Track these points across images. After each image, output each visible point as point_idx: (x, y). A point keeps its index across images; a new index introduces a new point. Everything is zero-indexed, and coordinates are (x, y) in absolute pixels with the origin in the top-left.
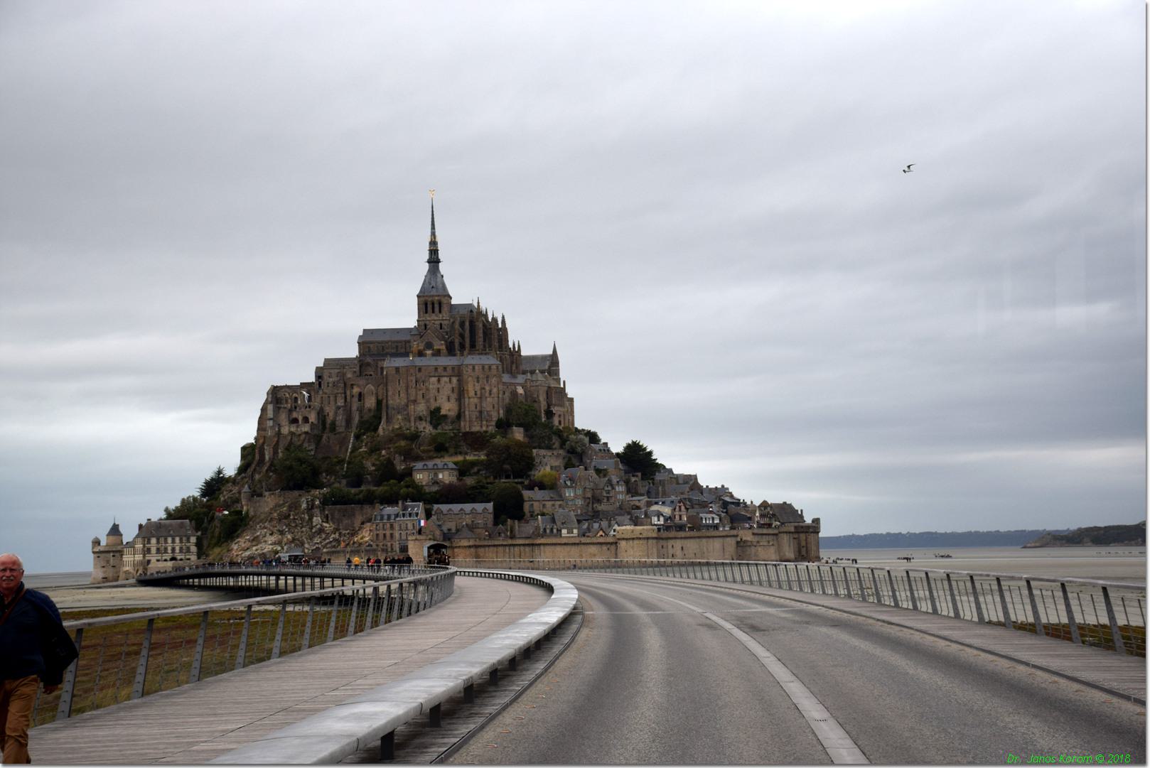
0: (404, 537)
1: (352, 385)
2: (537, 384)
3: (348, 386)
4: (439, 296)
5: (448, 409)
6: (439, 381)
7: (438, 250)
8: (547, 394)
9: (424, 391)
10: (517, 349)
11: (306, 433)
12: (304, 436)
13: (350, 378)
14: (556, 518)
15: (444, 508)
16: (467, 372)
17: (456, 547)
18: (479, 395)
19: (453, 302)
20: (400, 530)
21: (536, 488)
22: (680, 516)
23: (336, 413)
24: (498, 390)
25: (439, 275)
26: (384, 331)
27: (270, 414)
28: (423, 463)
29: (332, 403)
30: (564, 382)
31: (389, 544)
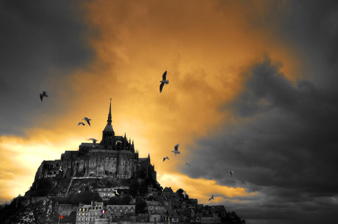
0: (92, 220)
2: (146, 163)
6: (109, 159)
8: (149, 168)
10: (137, 153)
11: (54, 177)
12: (53, 178)
13: (74, 157)
14: (169, 212)
15: (113, 206)
18: (125, 165)
19: (115, 135)
20: (90, 216)
21: (153, 200)
22: (223, 214)
23: (67, 171)
24: (132, 164)
27: (41, 171)
28: (102, 189)
29: (66, 167)
30: (154, 165)
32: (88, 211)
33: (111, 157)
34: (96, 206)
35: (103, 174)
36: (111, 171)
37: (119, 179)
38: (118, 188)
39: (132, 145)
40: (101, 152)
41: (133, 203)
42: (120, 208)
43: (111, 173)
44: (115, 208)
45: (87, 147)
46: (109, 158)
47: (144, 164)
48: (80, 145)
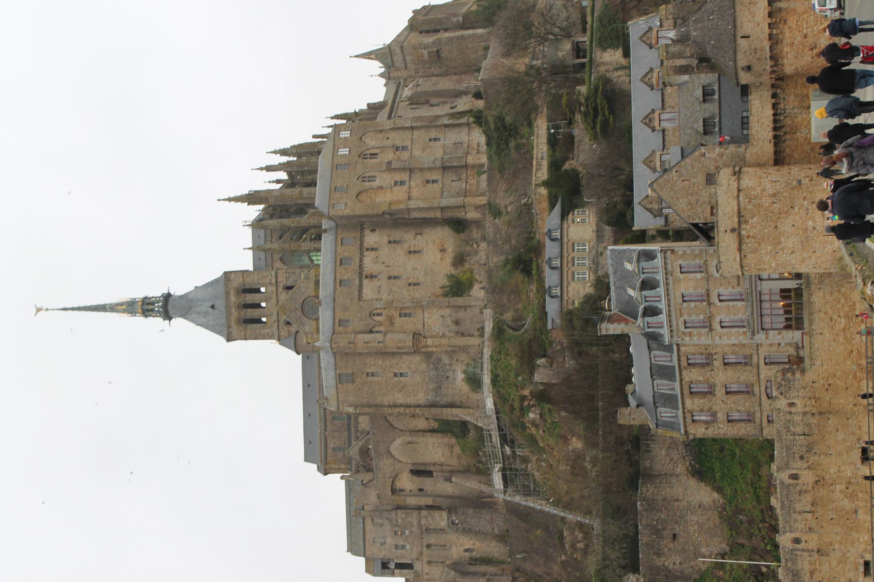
1: (394, 491)
2: (397, 50)
3: (399, 500)
4: (227, 293)
5: (439, 255)
6: (372, 277)
7: (146, 298)
8: (427, 32)
9: (396, 314)
10: (344, 122)
13: (379, 497)
16: (346, 207)
17: (775, 58)
18: (405, 176)
19: (251, 268)
20: (711, 330)
25: (191, 296)
26: (307, 415)
31: (766, 372)
32: (668, 348)
33: (361, 267)
34: (631, 292)
35: (465, 308)
36: (449, 258)
37: (489, 203)
38: (543, 191)
39: (298, 159)
40: (333, 334)
41: (623, 61)
42: (653, 130)
43: (459, 260)
44: (648, 162)
45: (326, 426)
46: (365, 282)
47: (402, 65)
48: (319, 469)
